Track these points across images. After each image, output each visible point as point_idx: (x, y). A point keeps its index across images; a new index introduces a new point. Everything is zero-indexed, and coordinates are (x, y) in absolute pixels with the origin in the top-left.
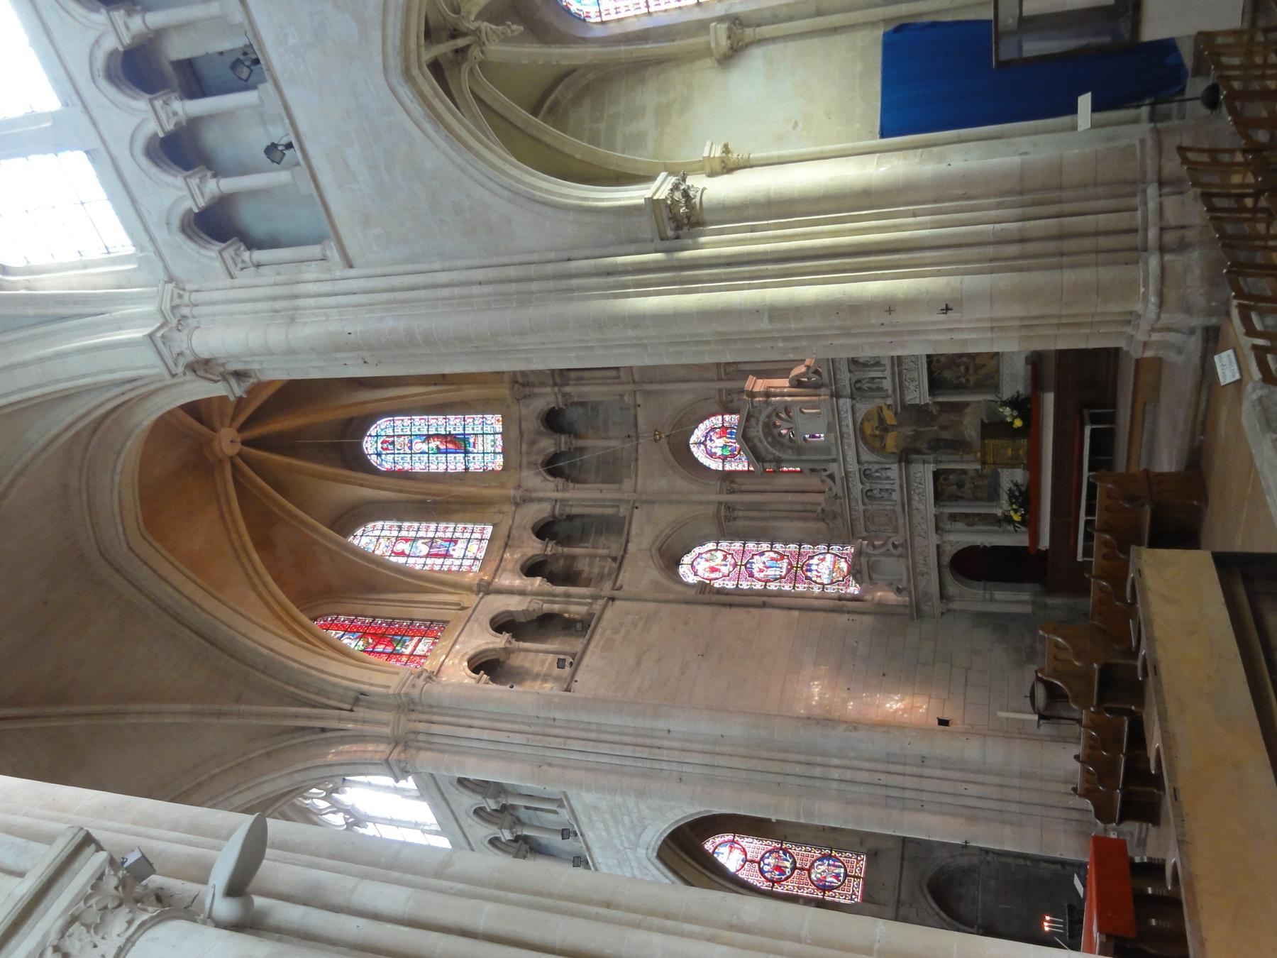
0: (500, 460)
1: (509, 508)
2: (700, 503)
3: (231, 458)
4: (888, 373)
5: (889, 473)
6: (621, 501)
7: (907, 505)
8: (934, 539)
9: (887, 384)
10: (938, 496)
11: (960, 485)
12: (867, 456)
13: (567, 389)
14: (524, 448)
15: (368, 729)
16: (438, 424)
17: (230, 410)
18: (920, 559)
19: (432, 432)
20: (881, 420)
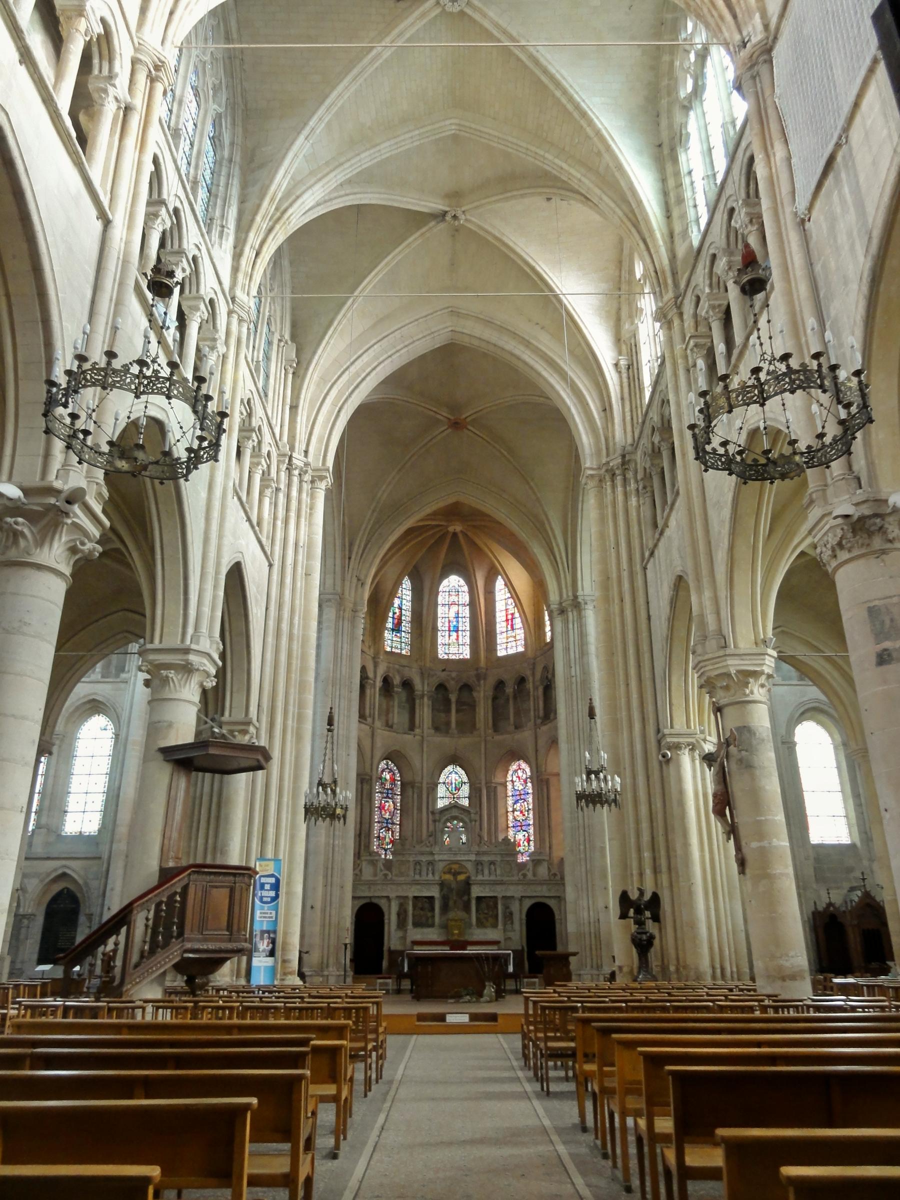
0: (388, 649)
2: (372, 765)
3: (447, 527)
4: (486, 878)
5: (430, 875)
6: (374, 719)
7: (416, 883)
8: (392, 895)
9: (480, 877)
10: (415, 898)
11: (422, 909)
13: (426, 699)
14: (397, 666)
15: (347, 584)
16: (407, 616)
17: (469, 534)
18: (379, 887)
19: (403, 612)
20: (459, 873)
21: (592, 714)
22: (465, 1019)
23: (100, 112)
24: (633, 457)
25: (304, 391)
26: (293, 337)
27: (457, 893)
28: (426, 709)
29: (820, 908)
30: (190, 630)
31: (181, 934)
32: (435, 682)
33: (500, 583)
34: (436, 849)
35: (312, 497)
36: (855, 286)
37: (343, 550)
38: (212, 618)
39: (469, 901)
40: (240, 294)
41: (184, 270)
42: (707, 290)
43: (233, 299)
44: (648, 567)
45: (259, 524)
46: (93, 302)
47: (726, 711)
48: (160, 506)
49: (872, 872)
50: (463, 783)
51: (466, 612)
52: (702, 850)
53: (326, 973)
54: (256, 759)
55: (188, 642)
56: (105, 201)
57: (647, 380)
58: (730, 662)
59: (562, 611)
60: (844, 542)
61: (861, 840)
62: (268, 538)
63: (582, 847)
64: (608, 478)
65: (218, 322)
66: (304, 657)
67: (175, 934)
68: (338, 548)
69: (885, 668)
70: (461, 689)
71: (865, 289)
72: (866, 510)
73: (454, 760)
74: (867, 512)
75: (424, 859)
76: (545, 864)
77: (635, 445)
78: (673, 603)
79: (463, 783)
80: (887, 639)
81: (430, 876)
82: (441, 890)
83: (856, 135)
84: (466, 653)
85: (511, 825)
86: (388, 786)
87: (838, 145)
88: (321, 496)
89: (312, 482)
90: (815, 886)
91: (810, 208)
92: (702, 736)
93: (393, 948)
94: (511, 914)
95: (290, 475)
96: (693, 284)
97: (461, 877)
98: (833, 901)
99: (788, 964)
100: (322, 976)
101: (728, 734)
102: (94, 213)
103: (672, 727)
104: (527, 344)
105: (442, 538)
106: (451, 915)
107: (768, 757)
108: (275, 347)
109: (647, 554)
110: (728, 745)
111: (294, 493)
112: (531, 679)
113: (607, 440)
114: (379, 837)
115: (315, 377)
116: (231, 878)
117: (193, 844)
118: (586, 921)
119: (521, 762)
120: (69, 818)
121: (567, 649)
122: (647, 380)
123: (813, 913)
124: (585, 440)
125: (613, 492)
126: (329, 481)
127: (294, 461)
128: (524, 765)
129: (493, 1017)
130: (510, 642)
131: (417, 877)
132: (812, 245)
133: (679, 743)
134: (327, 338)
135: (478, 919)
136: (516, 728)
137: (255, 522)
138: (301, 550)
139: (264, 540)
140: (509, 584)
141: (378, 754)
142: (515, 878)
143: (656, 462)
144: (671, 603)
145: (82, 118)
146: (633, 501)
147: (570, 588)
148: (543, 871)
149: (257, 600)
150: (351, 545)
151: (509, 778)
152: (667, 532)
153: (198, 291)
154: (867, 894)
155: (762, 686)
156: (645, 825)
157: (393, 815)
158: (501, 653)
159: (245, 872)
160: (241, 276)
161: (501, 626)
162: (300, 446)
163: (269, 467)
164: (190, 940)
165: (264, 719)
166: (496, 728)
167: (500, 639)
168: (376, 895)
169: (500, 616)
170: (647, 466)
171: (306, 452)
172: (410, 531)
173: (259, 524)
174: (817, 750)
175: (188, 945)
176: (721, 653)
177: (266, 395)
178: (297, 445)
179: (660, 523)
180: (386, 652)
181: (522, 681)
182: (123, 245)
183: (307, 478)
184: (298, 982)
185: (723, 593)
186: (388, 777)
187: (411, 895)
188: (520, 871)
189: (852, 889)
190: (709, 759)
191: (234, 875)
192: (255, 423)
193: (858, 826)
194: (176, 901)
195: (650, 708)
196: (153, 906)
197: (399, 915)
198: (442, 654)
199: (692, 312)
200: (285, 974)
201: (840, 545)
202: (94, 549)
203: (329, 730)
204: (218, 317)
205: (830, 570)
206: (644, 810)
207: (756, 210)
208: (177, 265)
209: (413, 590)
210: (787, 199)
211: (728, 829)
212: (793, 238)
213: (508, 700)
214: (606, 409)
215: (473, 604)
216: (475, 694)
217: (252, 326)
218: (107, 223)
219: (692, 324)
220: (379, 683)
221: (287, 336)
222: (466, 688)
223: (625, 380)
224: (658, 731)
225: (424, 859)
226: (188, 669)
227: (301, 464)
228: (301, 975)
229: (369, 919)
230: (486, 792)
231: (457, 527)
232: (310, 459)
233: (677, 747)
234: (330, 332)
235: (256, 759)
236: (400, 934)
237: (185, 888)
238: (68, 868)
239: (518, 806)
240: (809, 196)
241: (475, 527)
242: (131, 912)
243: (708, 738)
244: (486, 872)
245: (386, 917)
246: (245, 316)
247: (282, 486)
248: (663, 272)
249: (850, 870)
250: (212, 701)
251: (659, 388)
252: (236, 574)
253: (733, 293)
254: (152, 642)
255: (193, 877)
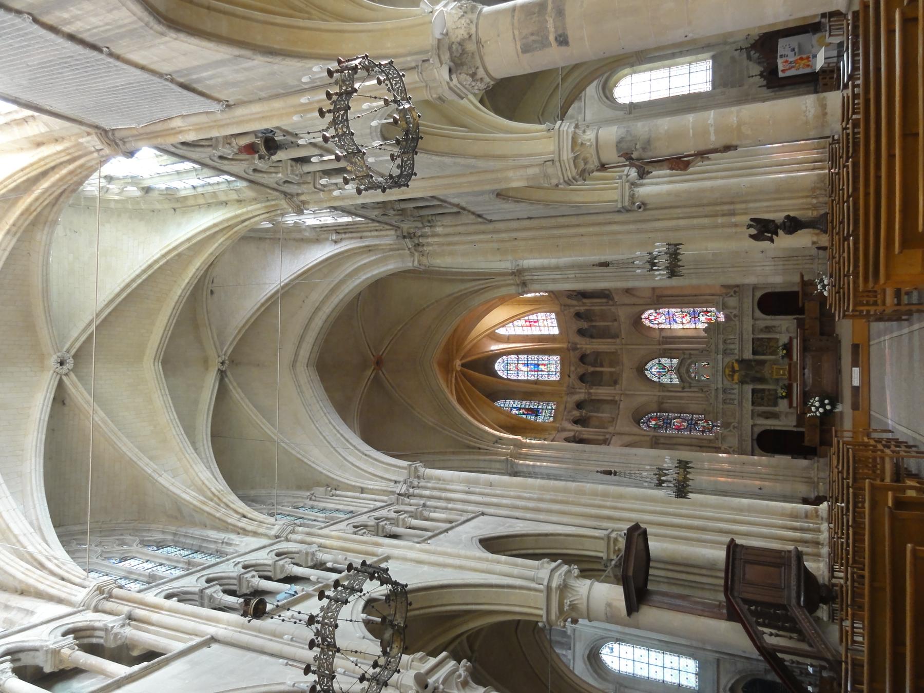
0: (551, 419)
1: (554, 433)
4: (737, 346)
5: (734, 391)
7: (741, 404)
8: (751, 422)
9: (736, 352)
10: (753, 404)
11: (763, 399)
12: (726, 382)
13: (592, 391)
16: (526, 404)
20: (733, 367)
21: (605, 264)
22: (856, 370)
23: (131, 639)
24: (405, 230)
25: (349, 482)
26: (308, 488)
27: (749, 371)
28: (599, 391)
29: (765, 83)
30: (533, 585)
31: (784, 607)
32: (578, 384)
33: (502, 331)
34: (713, 386)
35: (430, 479)
36: (276, 67)
37: (474, 453)
38: (522, 566)
39: (755, 361)
40: (273, 532)
41: (253, 576)
42: (280, 175)
43: (277, 537)
44: (489, 218)
45: (451, 522)
46: (272, 655)
47: (604, 160)
48: (434, 604)
49: (734, 43)
50: (659, 363)
51: (523, 358)
52: (716, 178)
53: (816, 479)
54: (637, 535)
55: (541, 587)
56: (198, 640)
57: (347, 219)
58: (565, 158)
59: (524, 284)
60: (471, 72)
61: (709, 51)
62: (461, 515)
63: (712, 270)
64: (420, 249)
65: (294, 550)
66: (555, 490)
67: (784, 612)
68: (472, 457)
69: (570, 40)
70: (584, 363)
71: (277, 59)
72: (446, 57)
73: (641, 370)
74: (447, 55)
75: (721, 396)
76: (726, 299)
77: (397, 228)
78: (517, 200)
79: (659, 363)
80: (547, 38)
81: (736, 391)
82: (747, 383)
83: (165, 68)
84: (555, 358)
85: (693, 326)
86: (661, 423)
87: (172, 81)
88: (430, 472)
89: (419, 477)
90: (746, 87)
91: (219, 101)
92: (624, 177)
93: (794, 423)
94: (767, 327)
95: (413, 495)
96: (275, 186)
97: (736, 366)
98: (758, 73)
99: (813, 111)
100: (818, 483)
101: (622, 159)
102: (205, 650)
103: (617, 201)
104: (318, 309)
105: (464, 375)
106: (767, 375)
107: (642, 128)
108: (315, 503)
109: (480, 220)
110: (632, 159)
111: (427, 493)
112: (577, 308)
113: (391, 250)
114: (703, 432)
115: (338, 473)
116: (737, 562)
117: (707, 587)
118: (773, 268)
119: (643, 317)
120: (684, 682)
121: (554, 281)
122: (347, 219)
123: (768, 88)
124: (391, 266)
125: (432, 245)
126: (418, 464)
127: (402, 491)
128: (645, 315)
129: (856, 348)
130: (547, 325)
131: (736, 402)
132: (246, 99)
133: (630, 196)
134: (310, 463)
135: (771, 354)
136: (615, 320)
137: (449, 525)
138: (472, 489)
139: (463, 519)
140: (503, 324)
141: (635, 430)
142: (737, 323)
143: (409, 212)
144: (518, 202)
145: (135, 653)
146: (439, 230)
147: (506, 278)
148: (732, 302)
149: (509, 527)
150: (469, 447)
151: (656, 326)
152: (463, 204)
153: (269, 565)
154: (754, 46)
155: (584, 132)
156: (695, 221)
157: (685, 420)
158: (555, 331)
159: (733, 548)
160: (260, 530)
161: (535, 331)
162: (391, 487)
163: (406, 512)
164: (789, 598)
165: (605, 524)
166: (616, 336)
167: (545, 332)
168: (750, 434)
169: (528, 332)
170: (412, 219)
171: (396, 482)
172: (460, 401)
173: (451, 522)
174: (636, 87)
175: (794, 601)
176: (558, 164)
177: (351, 512)
178: (390, 489)
179: (455, 210)
180: (554, 421)
181: (578, 315)
182: (230, 628)
183: (415, 483)
184: (824, 505)
185: (511, 163)
186: (654, 422)
187: (750, 407)
188: (731, 320)
189: (749, 58)
190: (642, 174)
191: (734, 559)
192: (372, 522)
193: (698, 54)
194: (756, 609)
195: (601, 218)
196: (760, 628)
197: (767, 418)
198: (555, 377)
199: (296, 187)
200: (817, 516)
201: (473, 75)
202: (465, 666)
203: (615, 475)
204: (290, 550)
205: (492, 83)
206: (682, 222)
207: (221, 141)
208: (249, 582)
209: (506, 398)
210: (212, 117)
211: (699, 159)
212: (240, 112)
213: (594, 327)
214: (369, 249)
215: (517, 353)
216: (588, 352)
217: (298, 522)
218: (213, 640)
219: (305, 186)
220: (578, 428)
221: (308, 494)
222: (583, 359)
223: (347, 235)
224: (619, 211)
225: (721, 396)
226: (564, 588)
227: (405, 487)
228: (818, 501)
229: (770, 442)
230: (667, 344)
231: (458, 363)
232: (402, 479)
233: (632, 196)
234: (305, 460)
235: (637, 535)
236: (783, 417)
237: (745, 601)
238: (726, 686)
239: (679, 320)
240: (209, 101)
241: (457, 351)
242: (764, 647)
243: (625, 173)
244: (732, 346)
245: (768, 428)
246: (291, 528)
247: (422, 502)
248: (266, 207)
249: (733, 59)
250: (590, 568)
251: (354, 210)
252: (491, 544)
253: (281, 155)
254: (541, 616)
255: (736, 594)
